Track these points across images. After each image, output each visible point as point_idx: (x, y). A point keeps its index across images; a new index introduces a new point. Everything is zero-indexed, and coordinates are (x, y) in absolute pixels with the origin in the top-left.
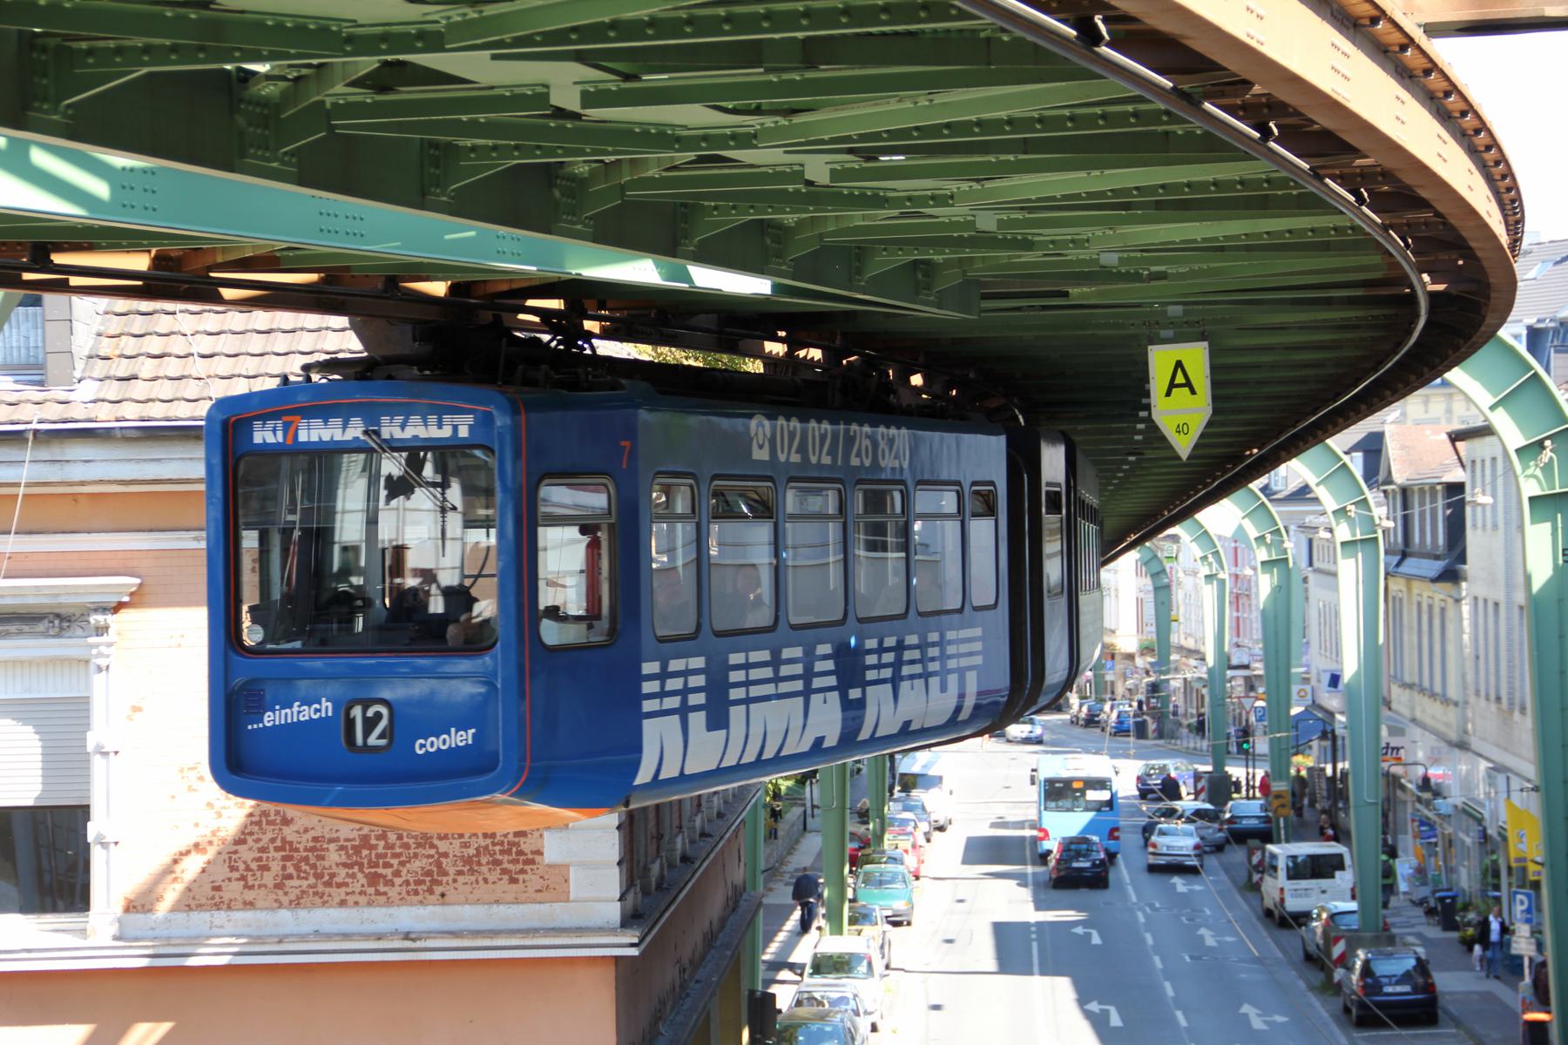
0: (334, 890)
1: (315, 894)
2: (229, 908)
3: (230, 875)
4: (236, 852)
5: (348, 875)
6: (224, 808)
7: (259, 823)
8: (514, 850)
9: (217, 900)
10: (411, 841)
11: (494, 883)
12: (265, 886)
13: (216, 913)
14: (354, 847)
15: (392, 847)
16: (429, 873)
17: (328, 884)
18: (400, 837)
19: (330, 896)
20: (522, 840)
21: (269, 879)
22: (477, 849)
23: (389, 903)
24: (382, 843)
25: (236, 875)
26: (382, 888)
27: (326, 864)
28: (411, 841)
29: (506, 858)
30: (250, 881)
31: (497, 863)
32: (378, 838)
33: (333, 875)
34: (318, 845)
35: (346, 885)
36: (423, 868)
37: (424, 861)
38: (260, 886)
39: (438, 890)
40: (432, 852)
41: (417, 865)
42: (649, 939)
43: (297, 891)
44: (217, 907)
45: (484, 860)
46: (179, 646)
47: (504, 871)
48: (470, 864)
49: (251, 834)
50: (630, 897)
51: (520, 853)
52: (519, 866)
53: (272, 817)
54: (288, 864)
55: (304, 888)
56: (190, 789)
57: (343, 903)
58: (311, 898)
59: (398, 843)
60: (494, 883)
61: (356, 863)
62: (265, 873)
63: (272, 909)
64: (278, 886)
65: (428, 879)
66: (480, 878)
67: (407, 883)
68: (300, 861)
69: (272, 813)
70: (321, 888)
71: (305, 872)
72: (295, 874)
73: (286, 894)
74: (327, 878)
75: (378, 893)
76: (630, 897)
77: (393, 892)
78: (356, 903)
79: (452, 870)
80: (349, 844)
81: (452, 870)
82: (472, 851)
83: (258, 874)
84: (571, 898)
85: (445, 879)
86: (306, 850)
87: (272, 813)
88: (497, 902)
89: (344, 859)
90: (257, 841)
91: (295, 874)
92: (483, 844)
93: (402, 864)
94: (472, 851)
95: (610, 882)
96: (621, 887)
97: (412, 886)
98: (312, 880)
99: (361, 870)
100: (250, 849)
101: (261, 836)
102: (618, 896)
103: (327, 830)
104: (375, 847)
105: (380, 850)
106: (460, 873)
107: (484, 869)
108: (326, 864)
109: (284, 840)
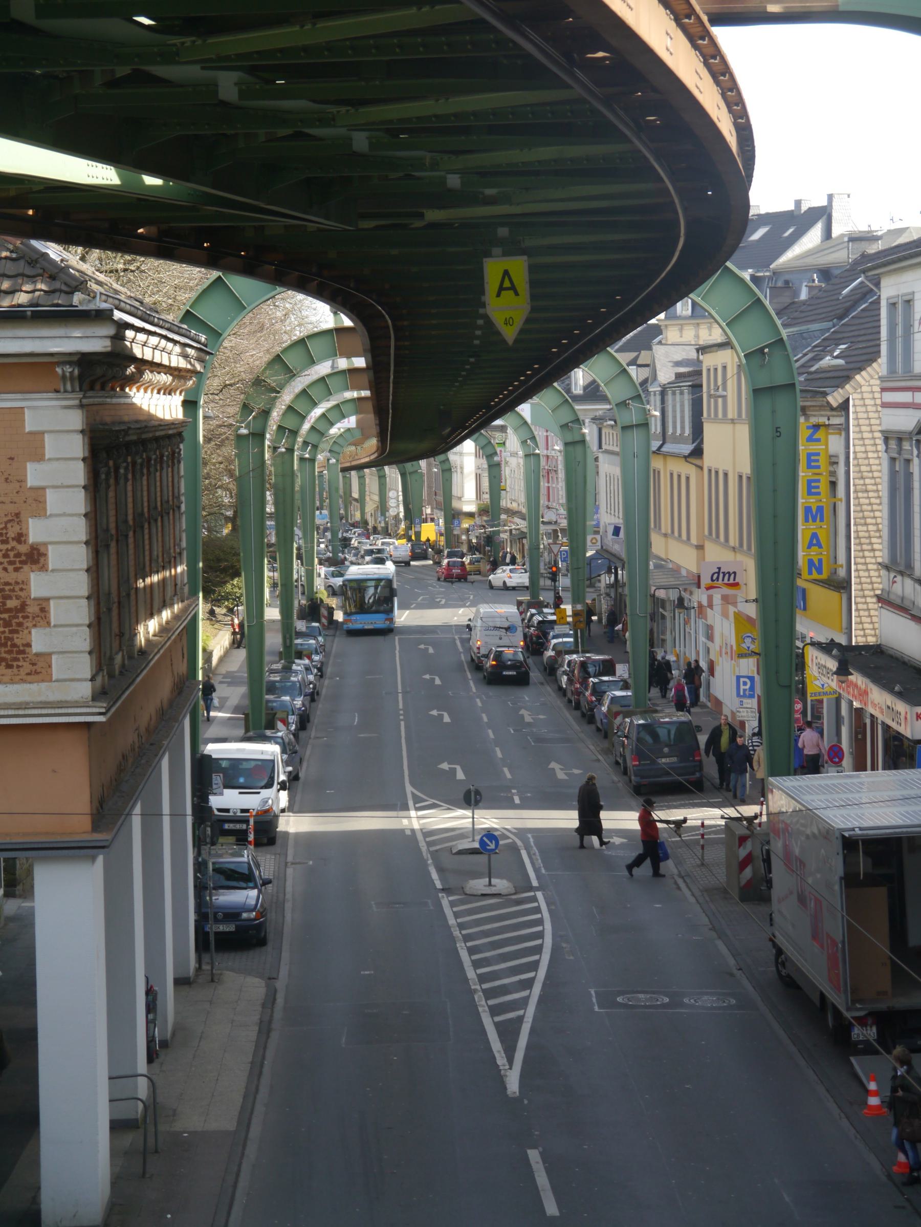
8: (9, 643)
20: (15, 636)
42: (113, 710)
50: (99, 679)
51: (14, 645)
76: (99, 679)
84: (54, 679)
95: (84, 666)
96: (92, 670)
102: (89, 677)
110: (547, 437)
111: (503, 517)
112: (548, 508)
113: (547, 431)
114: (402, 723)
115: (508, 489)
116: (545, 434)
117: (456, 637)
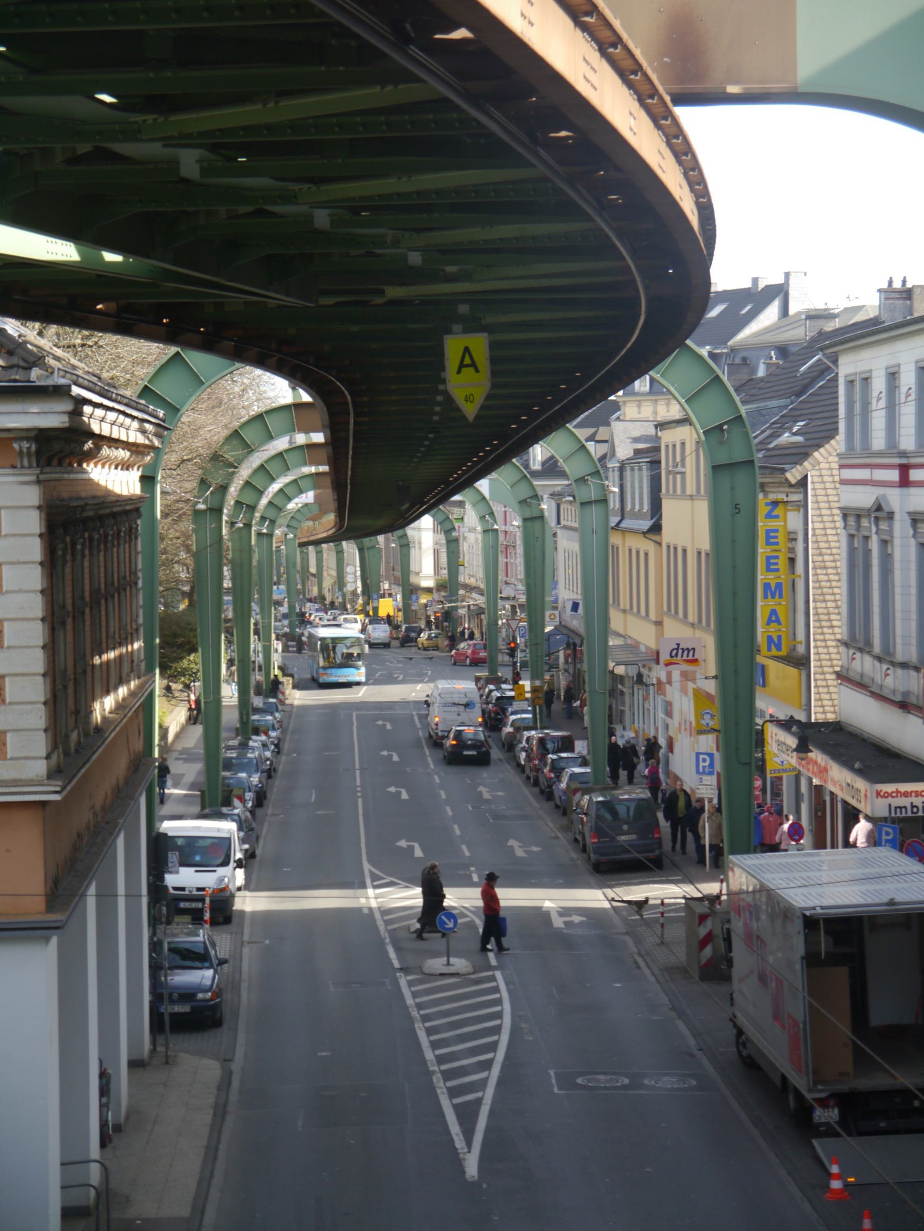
42: (69, 788)
50: (54, 757)
76: (54, 757)
84: (8, 757)
95: (39, 744)
96: (47, 749)
102: (44, 755)
110: (505, 512)
111: (461, 592)
112: (507, 583)
113: (505, 507)
114: (360, 800)
115: (466, 565)
116: (503, 509)
117: (414, 713)
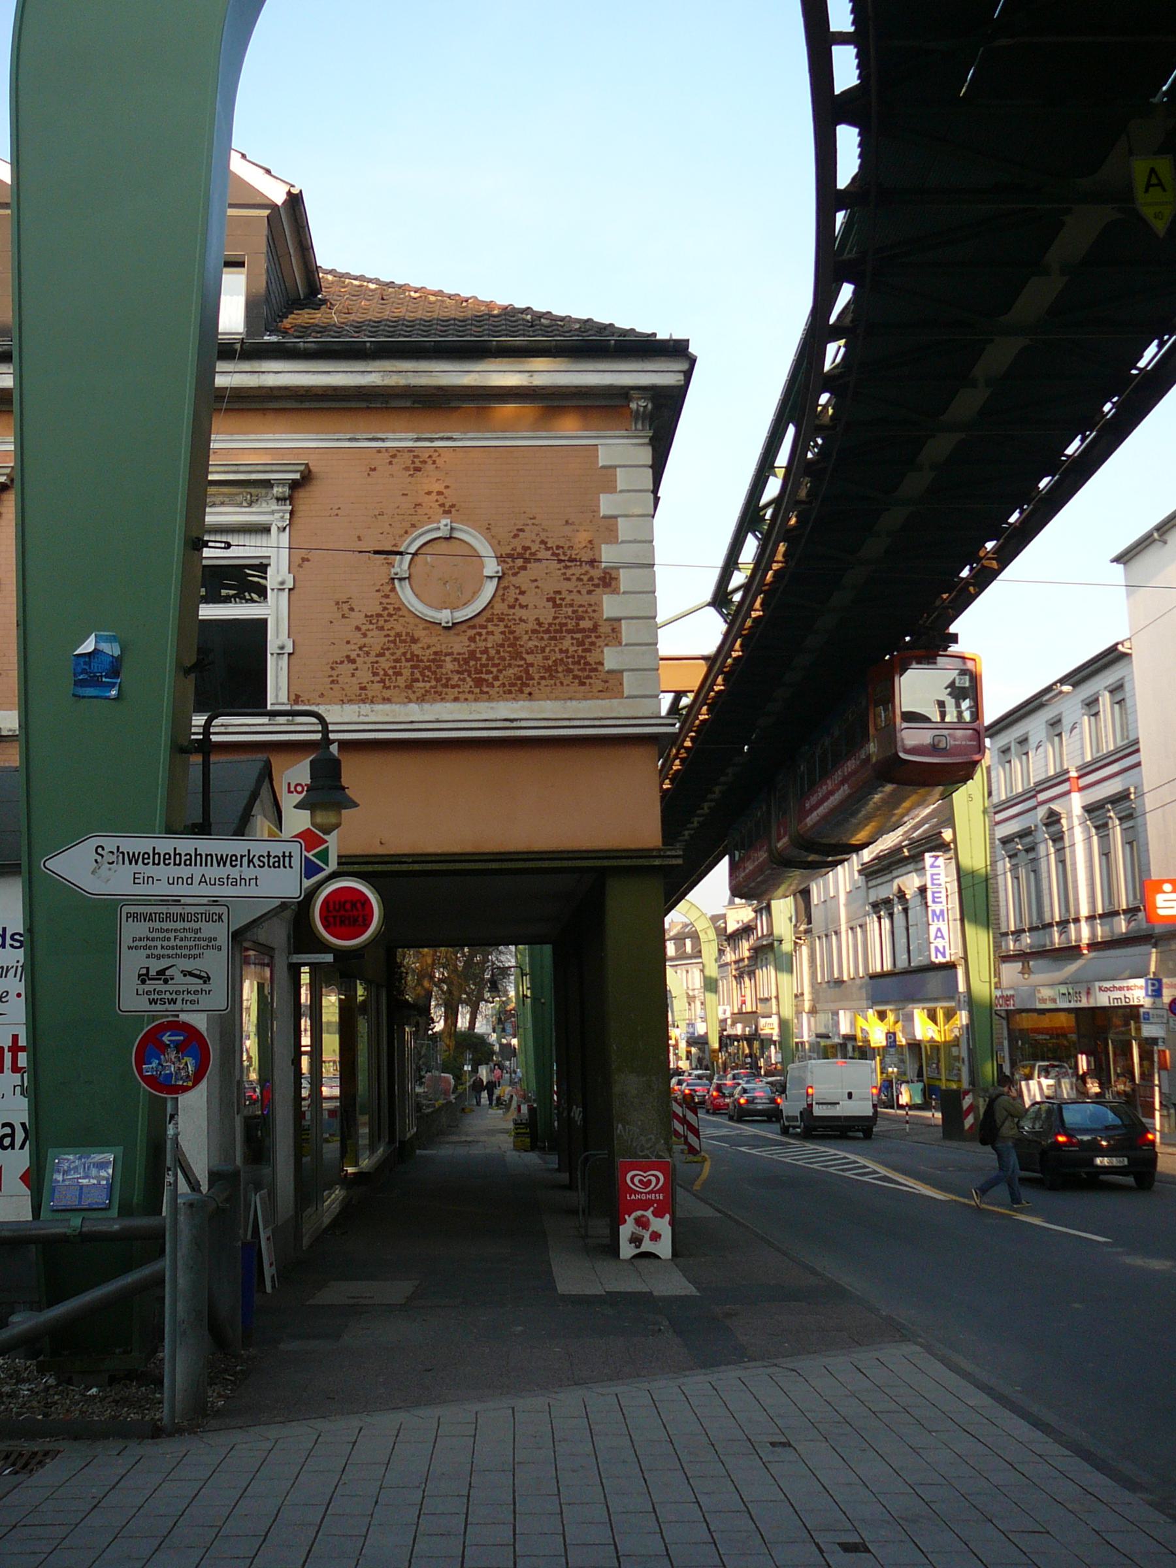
0: (449, 690)
1: (436, 692)
2: (372, 702)
3: (373, 679)
4: (377, 662)
5: (460, 679)
6: (368, 630)
7: (394, 642)
8: (582, 661)
9: (363, 696)
10: (506, 655)
11: (568, 685)
12: (399, 687)
13: (362, 706)
14: (463, 659)
15: (492, 659)
16: (520, 678)
17: (446, 686)
18: (498, 652)
19: (446, 694)
20: (588, 654)
21: (401, 681)
22: (554, 661)
23: (490, 699)
24: (485, 656)
25: (378, 678)
26: (485, 689)
27: (444, 671)
28: (506, 655)
29: (576, 667)
30: (388, 684)
31: (570, 671)
32: (482, 652)
33: (448, 679)
34: (438, 657)
35: (459, 686)
36: (515, 674)
37: (516, 669)
38: (395, 687)
39: (527, 690)
40: (522, 663)
41: (511, 672)
43: (423, 691)
44: (364, 701)
45: (560, 669)
46: (337, 515)
47: (575, 677)
48: (550, 671)
49: (388, 649)
51: (587, 663)
52: (586, 673)
53: (404, 638)
54: (416, 671)
55: (427, 688)
56: (343, 616)
57: (456, 699)
58: (433, 695)
59: (497, 656)
60: (568, 685)
61: (466, 670)
62: (399, 678)
63: (404, 703)
64: (409, 687)
65: (519, 682)
66: (558, 681)
67: (504, 685)
68: (424, 669)
69: (404, 634)
70: (439, 689)
71: (428, 676)
72: (421, 679)
73: (414, 692)
74: (444, 681)
75: (482, 692)
77: (492, 692)
78: (466, 700)
79: (537, 676)
80: (461, 657)
81: (537, 676)
82: (550, 662)
83: (394, 678)
85: (531, 682)
86: (429, 661)
87: (404, 634)
88: (570, 699)
89: (457, 668)
90: (393, 654)
91: (421, 679)
92: (559, 657)
93: (500, 671)
94: (550, 662)
97: (508, 688)
98: (433, 683)
99: (469, 675)
100: (387, 660)
101: (396, 651)
103: (444, 646)
104: (480, 659)
105: (484, 661)
106: (543, 678)
107: (560, 675)
108: (444, 671)
109: (412, 653)
